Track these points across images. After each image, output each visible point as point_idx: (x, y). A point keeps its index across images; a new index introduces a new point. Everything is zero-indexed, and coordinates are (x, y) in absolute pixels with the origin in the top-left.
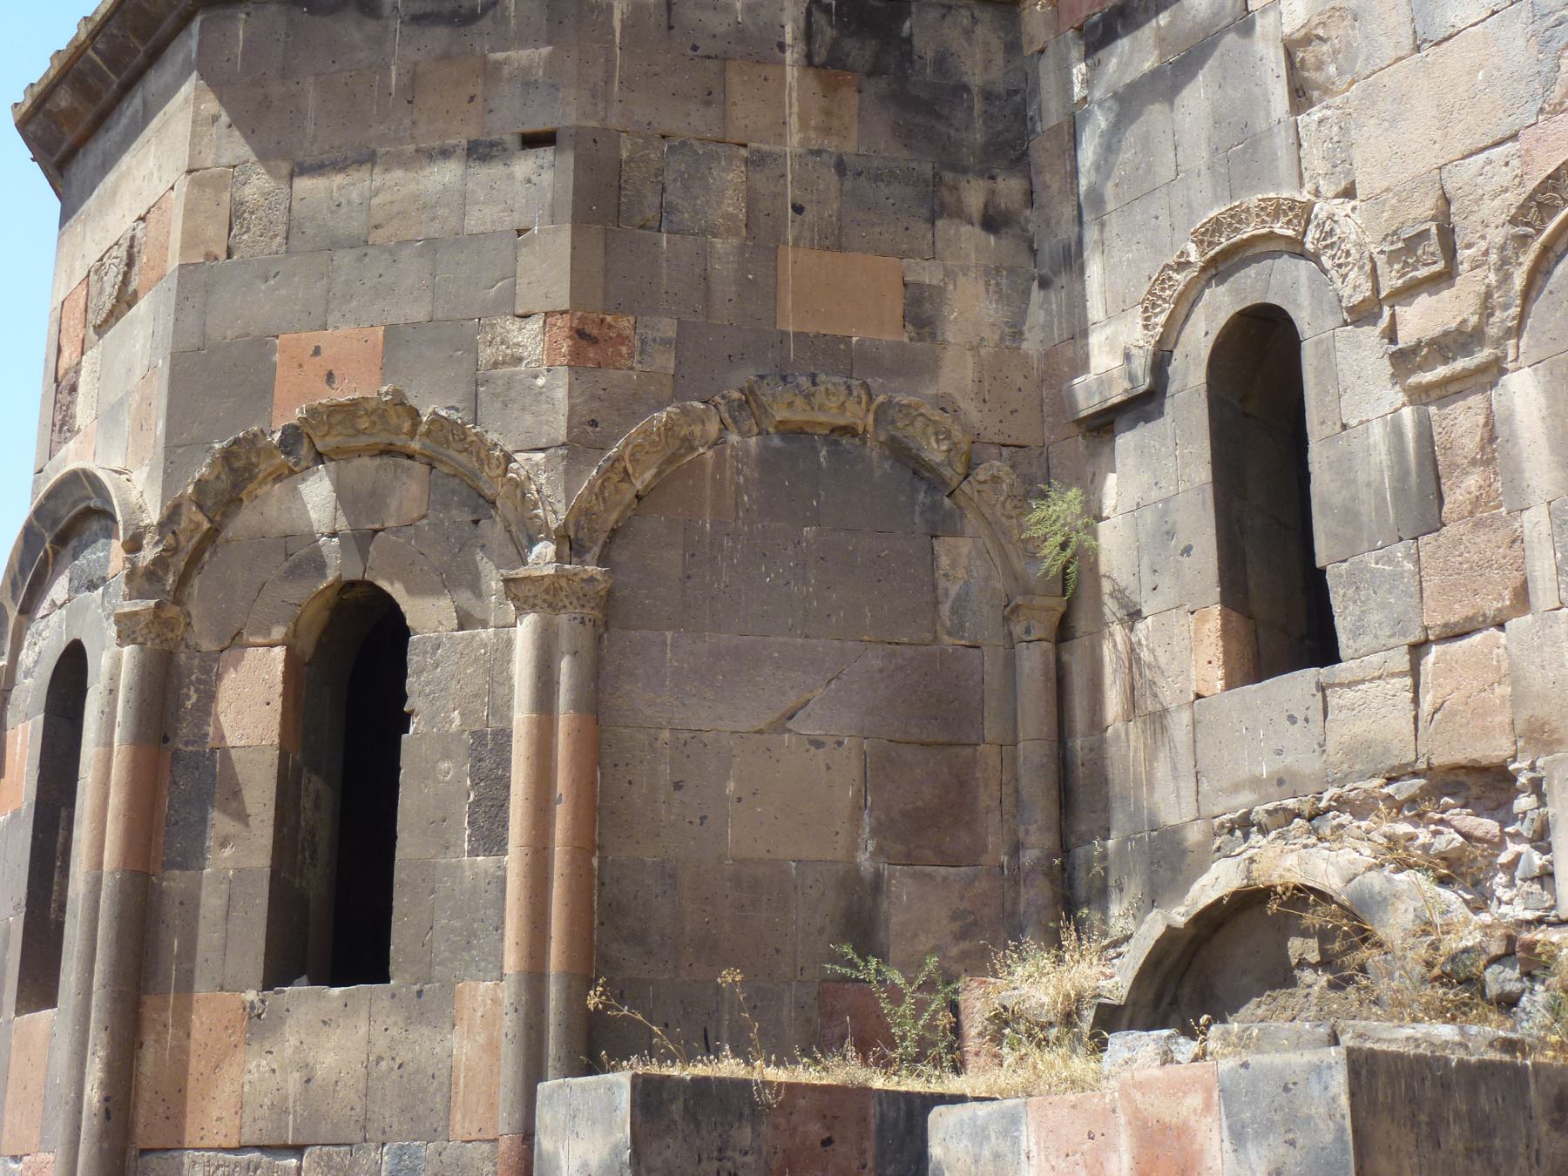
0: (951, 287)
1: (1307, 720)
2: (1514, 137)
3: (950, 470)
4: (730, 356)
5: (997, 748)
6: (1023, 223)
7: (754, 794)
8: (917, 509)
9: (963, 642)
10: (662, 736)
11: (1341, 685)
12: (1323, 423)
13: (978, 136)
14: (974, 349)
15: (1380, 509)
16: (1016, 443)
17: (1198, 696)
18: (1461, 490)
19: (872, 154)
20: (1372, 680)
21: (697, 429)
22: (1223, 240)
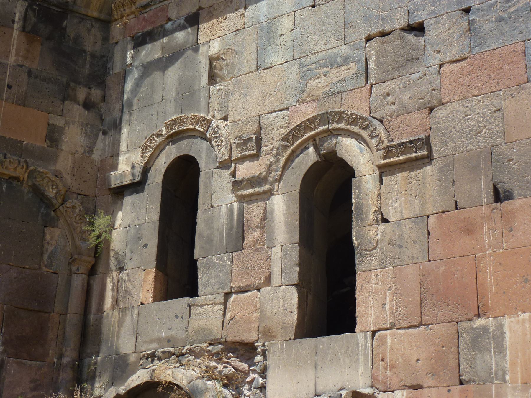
0: (67, 128)
1: (182, 318)
2: (287, 109)
3: (56, 200)
5: (59, 315)
6: (99, 108)
8: (40, 214)
9: (51, 271)
11: (197, 305)
12: (204, 204)
13: (87, 71)
14: (73, 154)
15: (221, 240)
16: (84, 194)
17: (142, 304)
18: (252, 236)
19: (43, 70)
20: (209, 305)
22: (176, 128)
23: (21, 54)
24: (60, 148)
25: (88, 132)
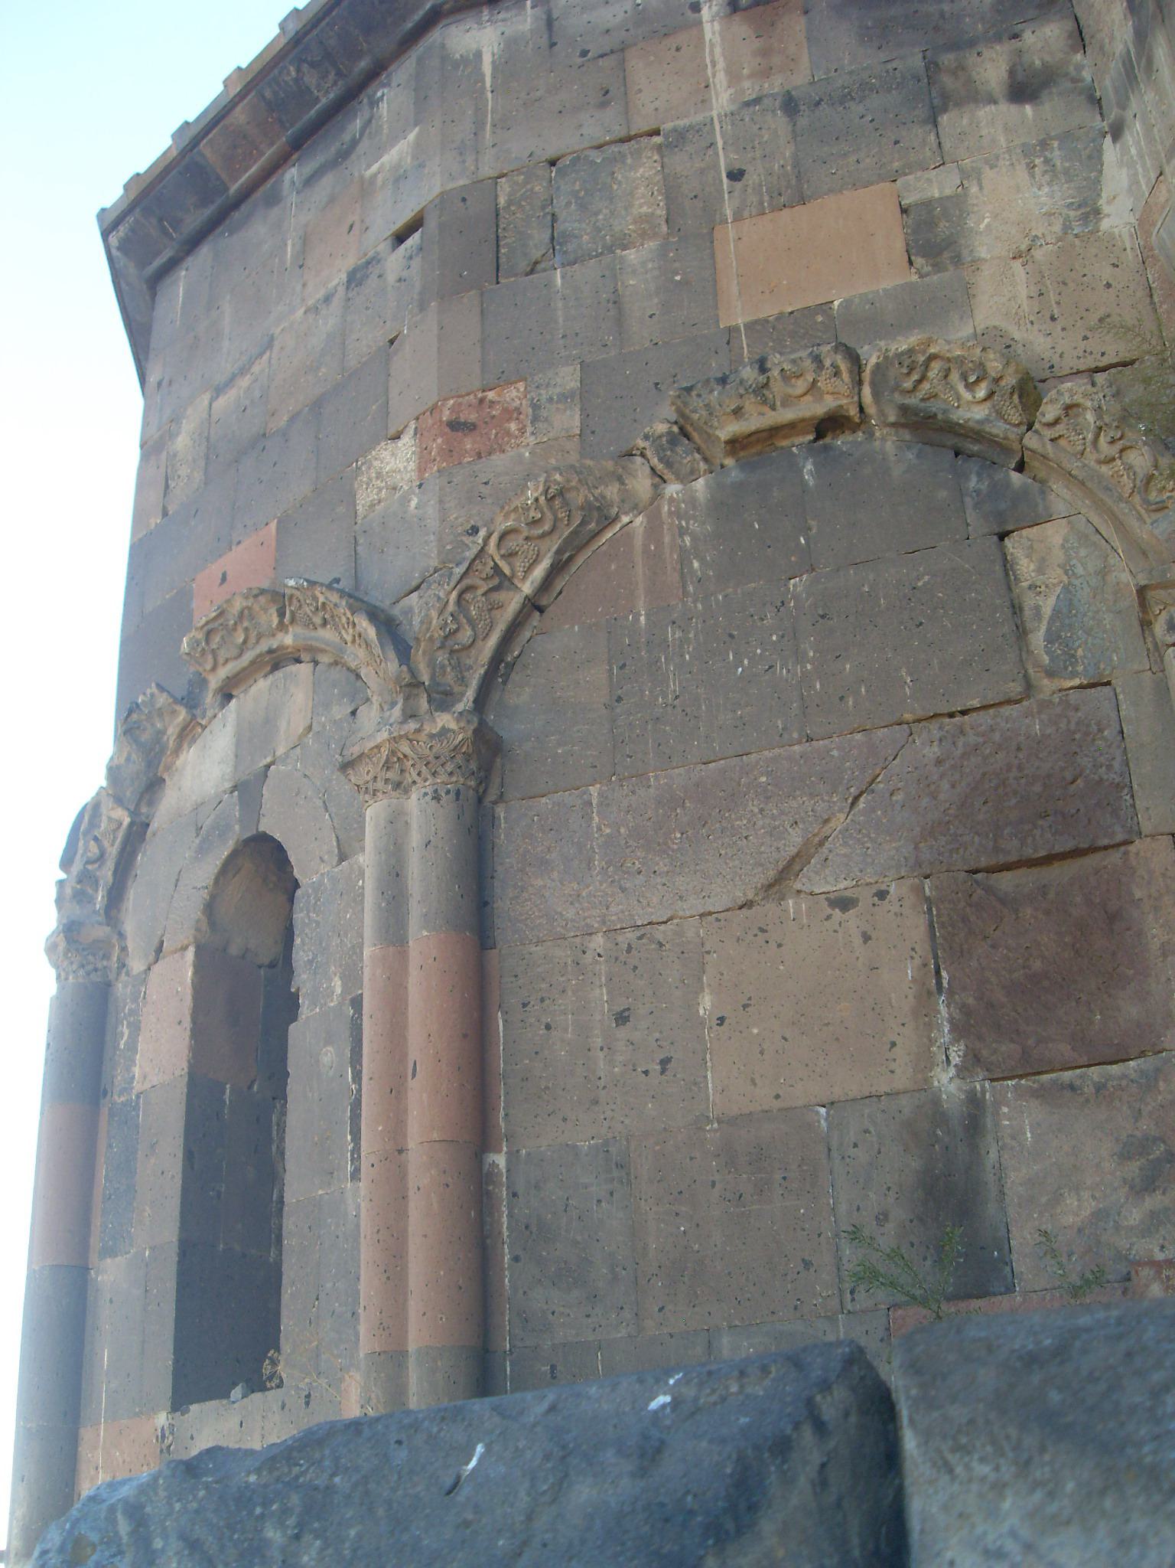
0: (974, 189)
3: (1001, 424)
4: (657, 384)
7: (745, 1006)
9: (1077, 682)
10: (592, 945)
16: (1115, 360)
21: (612, 491)
23: (745, 72)
24: (970, 259)
25: (1058, 164)
